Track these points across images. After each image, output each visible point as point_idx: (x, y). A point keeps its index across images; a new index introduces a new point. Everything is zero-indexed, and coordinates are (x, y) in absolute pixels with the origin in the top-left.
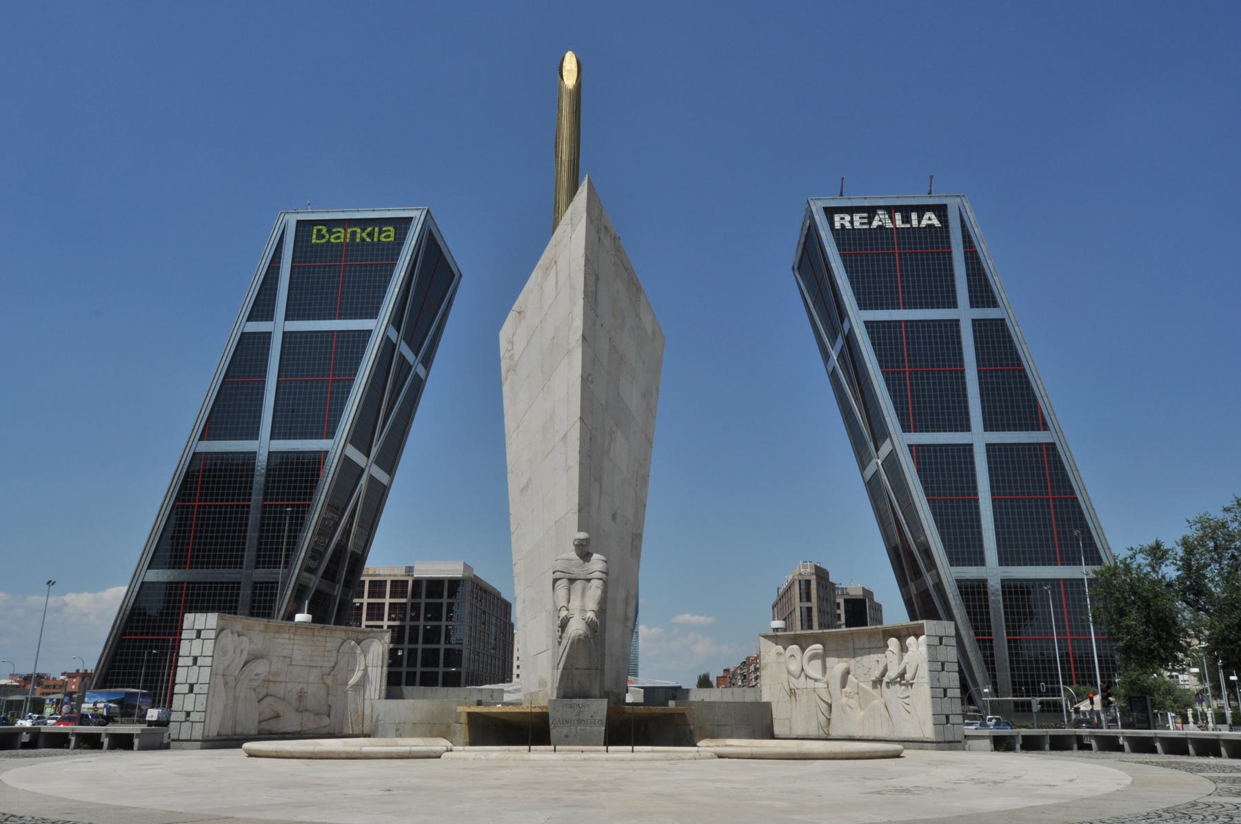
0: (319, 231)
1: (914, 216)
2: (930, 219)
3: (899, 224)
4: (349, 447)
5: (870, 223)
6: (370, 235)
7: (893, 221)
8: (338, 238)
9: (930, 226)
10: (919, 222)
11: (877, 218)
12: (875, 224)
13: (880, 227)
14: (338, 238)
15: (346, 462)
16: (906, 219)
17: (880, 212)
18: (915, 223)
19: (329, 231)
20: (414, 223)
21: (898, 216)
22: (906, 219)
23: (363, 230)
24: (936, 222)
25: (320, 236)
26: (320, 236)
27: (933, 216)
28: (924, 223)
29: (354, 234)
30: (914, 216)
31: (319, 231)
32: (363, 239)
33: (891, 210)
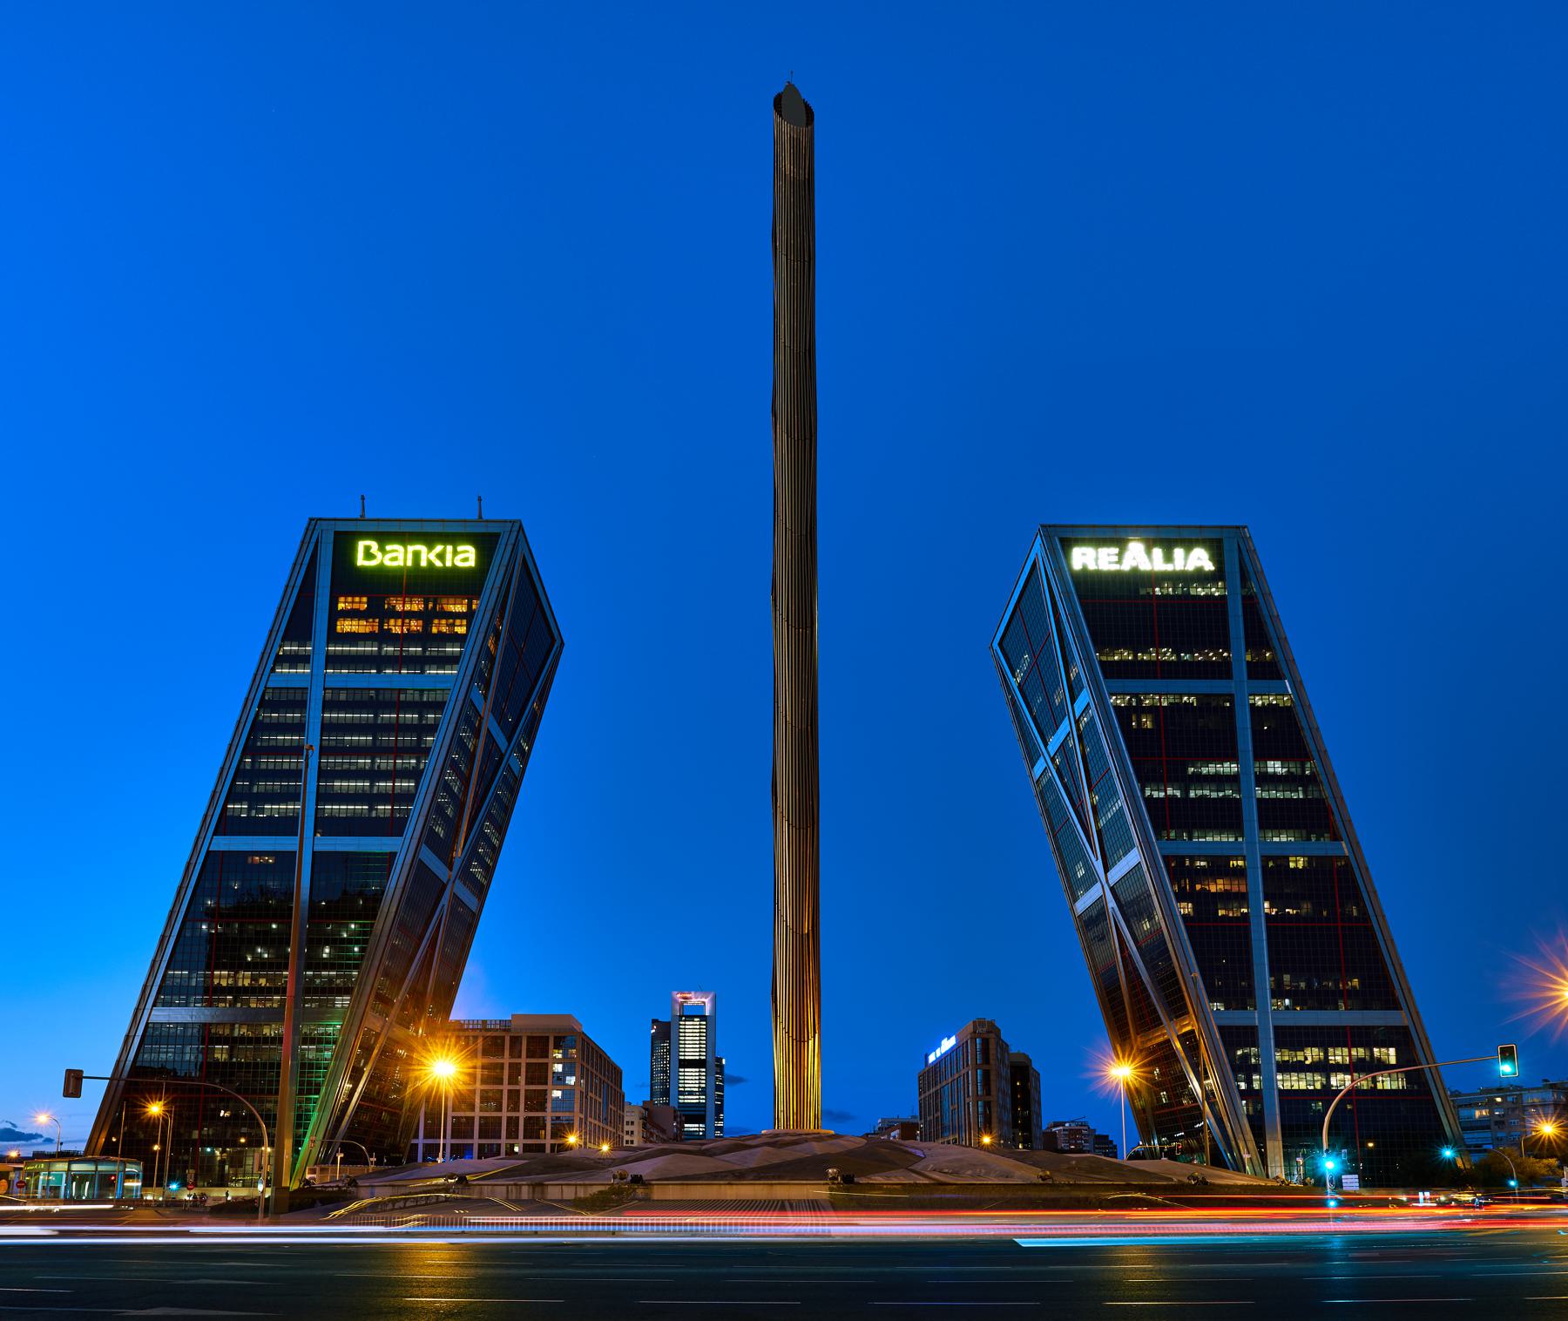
0: (367, 549)
4: (424, 848)
5: (1120, 562)
6: (441, 556)
8: (395, 559)
12: (1126, 566)
14: (395, 559)
15: (420, 871)
16: (1169, 558)
19: (382, 549)
20: (502, 541)
22: (1169, 558)
23: (430, 548)
25: (369, 555)
26: (369, 555)
29: (417, 555)
31: (367, 549)
32: (430, 563)
33: (1150, 544)
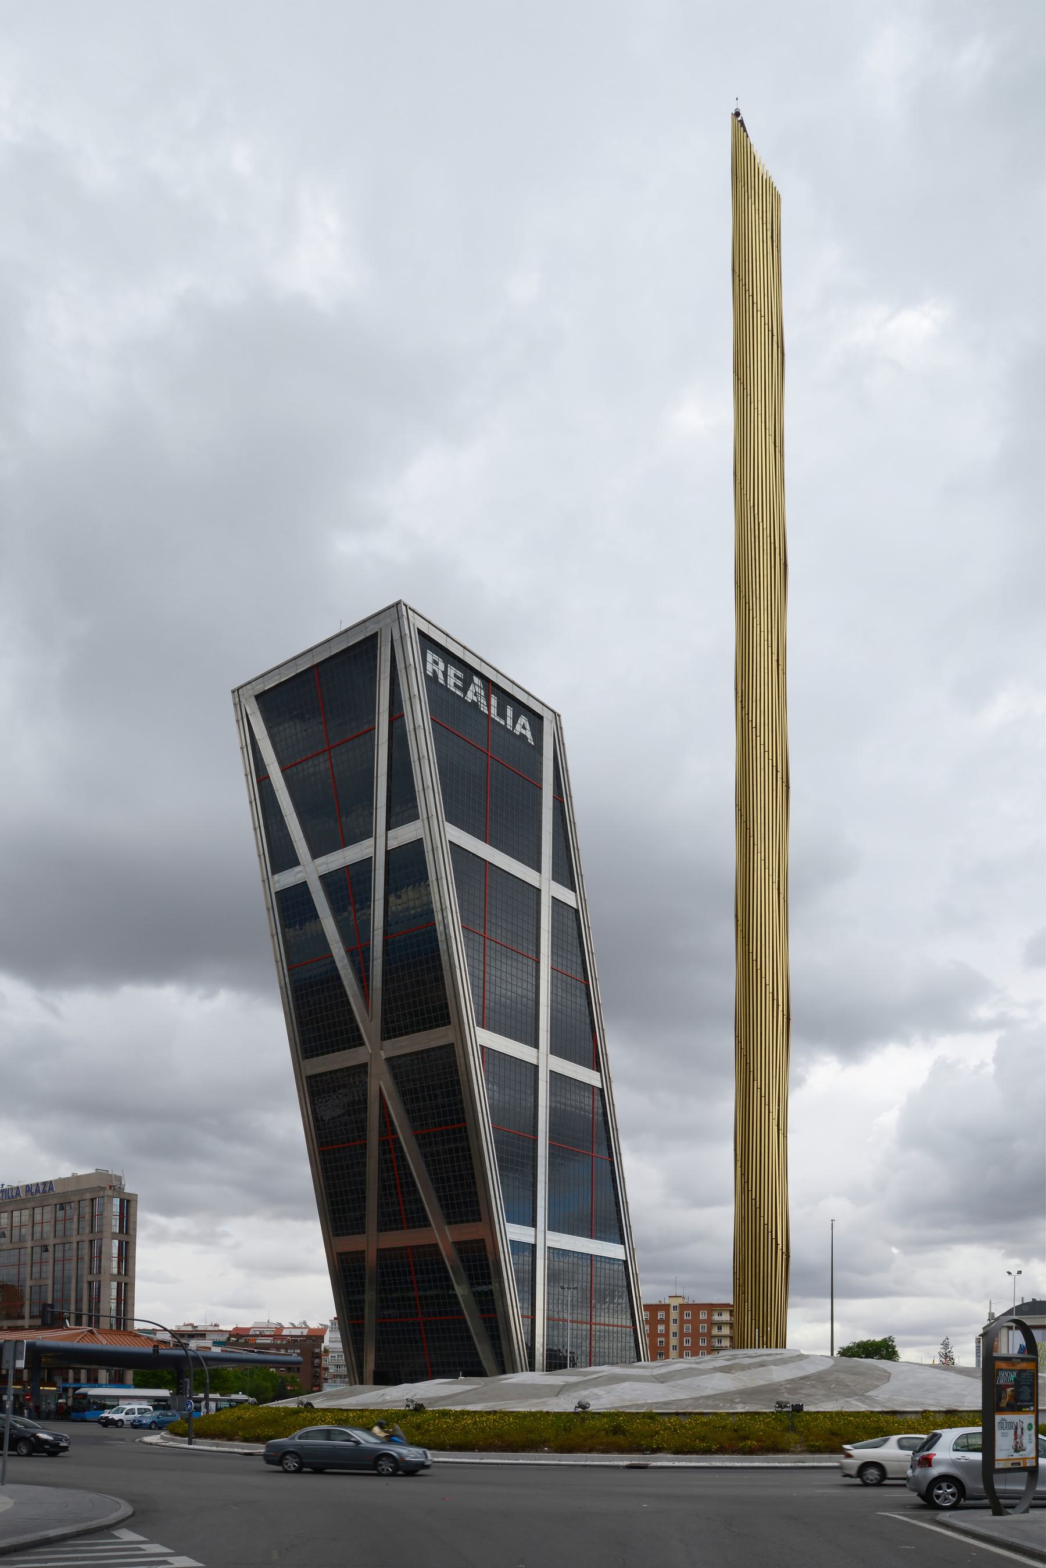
1: (509, 712)
2: (522, 727)
3: (494, 711)
7: (489, 706)
9: (523, 737)
10: (514, 726)
11: (472, 687)
12: (470, 696)
13: (475, 705)
17: (476, 680)
18: (510, 722)
21: (494, 701)
22: (502, 714)
24: (528, 734)
27: (528, 727)
28: (518, 729)
30: (509, 712)
